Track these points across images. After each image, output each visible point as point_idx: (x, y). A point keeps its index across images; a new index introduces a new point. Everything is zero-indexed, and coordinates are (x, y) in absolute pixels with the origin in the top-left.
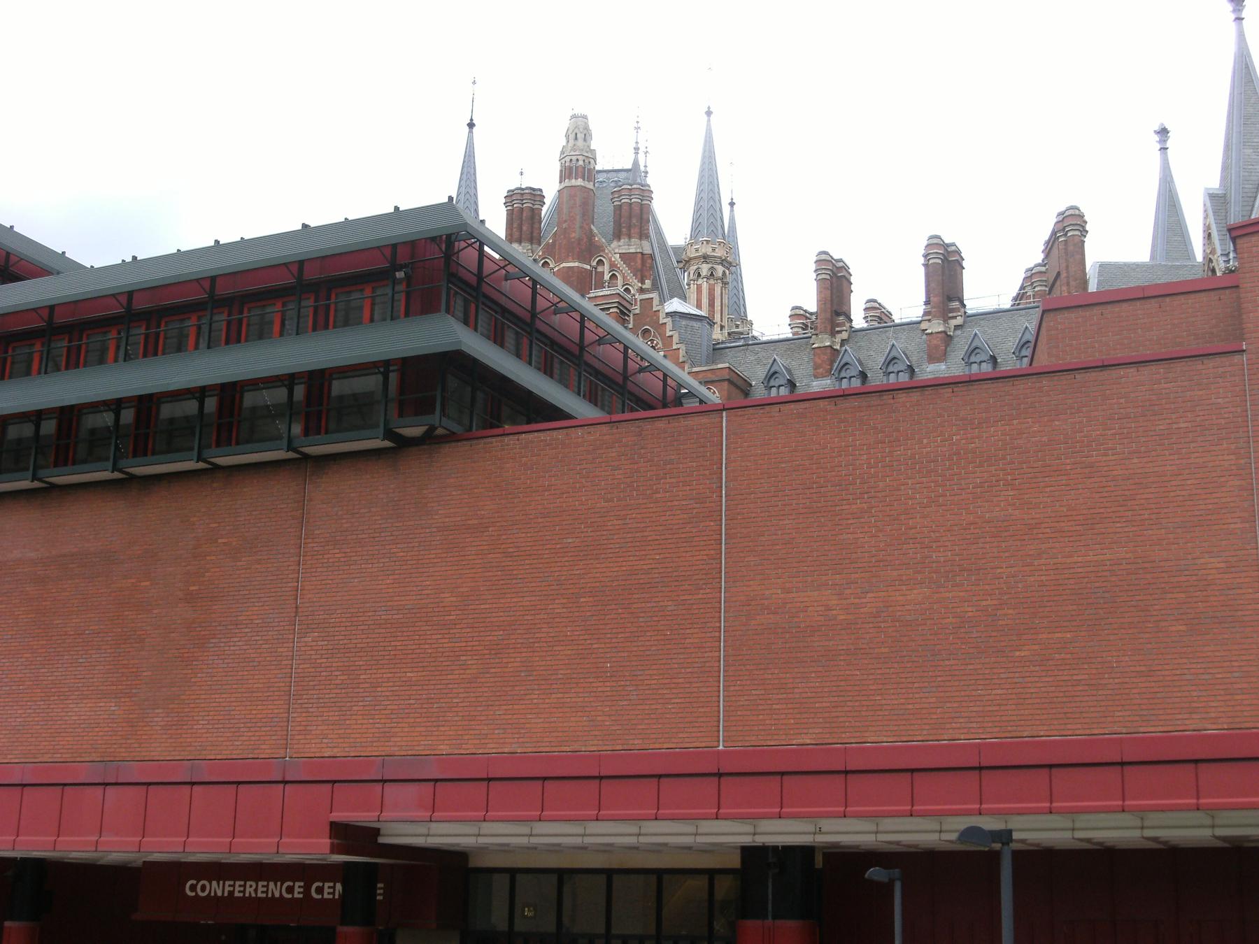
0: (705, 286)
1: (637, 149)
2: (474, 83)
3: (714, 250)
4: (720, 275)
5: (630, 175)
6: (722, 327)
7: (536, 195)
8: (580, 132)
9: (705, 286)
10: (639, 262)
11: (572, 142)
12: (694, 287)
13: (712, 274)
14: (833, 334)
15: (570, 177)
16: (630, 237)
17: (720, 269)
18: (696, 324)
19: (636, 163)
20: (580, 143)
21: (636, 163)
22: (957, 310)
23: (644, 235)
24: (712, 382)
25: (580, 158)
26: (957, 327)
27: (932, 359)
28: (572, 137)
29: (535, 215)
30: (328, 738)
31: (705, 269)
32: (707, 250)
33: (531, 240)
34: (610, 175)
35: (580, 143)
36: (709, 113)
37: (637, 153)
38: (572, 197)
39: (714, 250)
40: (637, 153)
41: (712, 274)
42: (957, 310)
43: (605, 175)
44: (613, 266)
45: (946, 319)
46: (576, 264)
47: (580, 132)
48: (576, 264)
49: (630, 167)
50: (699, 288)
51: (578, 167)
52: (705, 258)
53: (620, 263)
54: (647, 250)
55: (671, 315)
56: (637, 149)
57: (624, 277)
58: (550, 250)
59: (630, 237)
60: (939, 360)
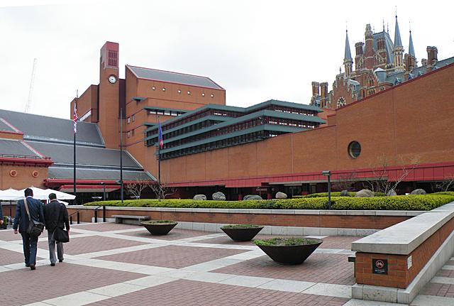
7: (361, 44)
8: (368, 27)
30: (261, 173)
31: (397, 53)
32: (397, 49)
47: (368, 27)
51: (369, 34)
52: (397, 51)
54: (385, 50)
58: (365, 55)
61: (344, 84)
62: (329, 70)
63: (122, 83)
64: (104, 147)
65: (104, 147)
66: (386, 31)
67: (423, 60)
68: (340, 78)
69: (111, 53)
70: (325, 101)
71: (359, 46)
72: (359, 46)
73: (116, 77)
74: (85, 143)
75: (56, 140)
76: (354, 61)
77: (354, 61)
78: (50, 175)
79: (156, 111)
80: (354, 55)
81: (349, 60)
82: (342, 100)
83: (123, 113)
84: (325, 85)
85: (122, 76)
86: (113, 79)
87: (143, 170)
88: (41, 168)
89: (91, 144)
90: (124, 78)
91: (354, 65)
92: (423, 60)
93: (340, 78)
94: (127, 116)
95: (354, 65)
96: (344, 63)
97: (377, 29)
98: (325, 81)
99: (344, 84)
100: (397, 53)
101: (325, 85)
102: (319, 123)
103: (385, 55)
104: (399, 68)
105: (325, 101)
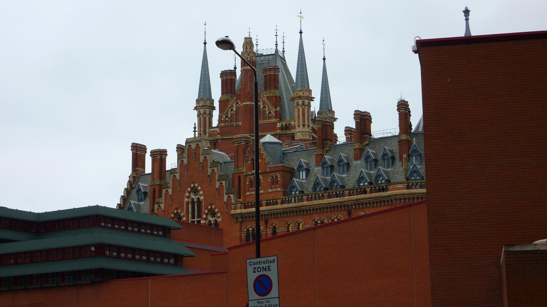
0: (301, 109)
1: (277, 45)
2: (205, 24)
3: (303, 93)
4: (307, 104)
5: (274, 57)
6: (308, 126)
7: (232, 73)
9: (301, 109)
10: (274, 100)
11: (245, 50)
12: (296, 110)
13: (303, 104)
14: (323, 148)
15: (244, 66)
16: (270, 89)
17: (306, 102)
18: (275, 146)
19: (277, 51)
20: (249, 50)
21: (277, 51)
22: (366, 138)
23: (277, 87)
24: (277, 171)
25: (249, 57)
26: (366, 145)
27: (356, 159)
28: (245, 47)
29: (233, 81)
31: (300, 103)
32: (301, 94)
33: (231, 92)
34: (266, 57)
35: (249, 50)
36: (301, 33)
37: (277, 47)
38: (246, 74)
39: (303, 93)
40: (277, 47)
41: (303, 104)
42: (366, 138)
43: (264, 57)
44: (264, 103)
45: (361, 143)
46: (249, 103)
48: (249, 103)
49: (273, 52)
50: (299, 109)
51: (250, 57)
52: (300, 97)
53: (267, 101)
54: (277, 93)
55: (264, 143)
56: (277, 45)
57: (268, 107)
58: (238, 98)
59: (270, 89)
60: (358, 160)
61: (202, 158)
62: (172, 129)
66: (280, 49)
67: (348, 131)
68: (193, 146)
70: (161, 187)
71: (227, 77)
72: (227, 77)
76: (216, 104)
77: (216, 104)
80: (216, 93)
81: (208, 103)
82: (195, 191)
84: (160, 156)
91: (216, 114)
92: (348, 131)
93: (193, 146)
95: (216, 114)
96: (196, 108)
97: (264, 46)
98: (162, 148)
99: (202, 158)
100: (300, 102)
101: (160, 156)
102: (182, 256)
103: (277, 101)
104: (302, 132)
105: (160, 186)
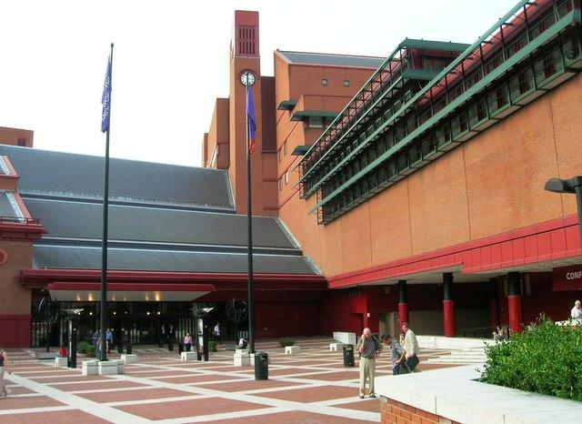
63: (269, 85)
64: (234, 212)
65: (234, 212)
69: (247, 28)
73: (254, 70)
74: (193, 206)
75: (130, 200)
78: (40, 256)
79: (325, 120)
83: (270, 144)
85: (267, 69)
86: (248, 79)
87: (300, 253)
88: (14, 244)
89: (206, 207)
90: (273, 76)
94: (280, 142)
